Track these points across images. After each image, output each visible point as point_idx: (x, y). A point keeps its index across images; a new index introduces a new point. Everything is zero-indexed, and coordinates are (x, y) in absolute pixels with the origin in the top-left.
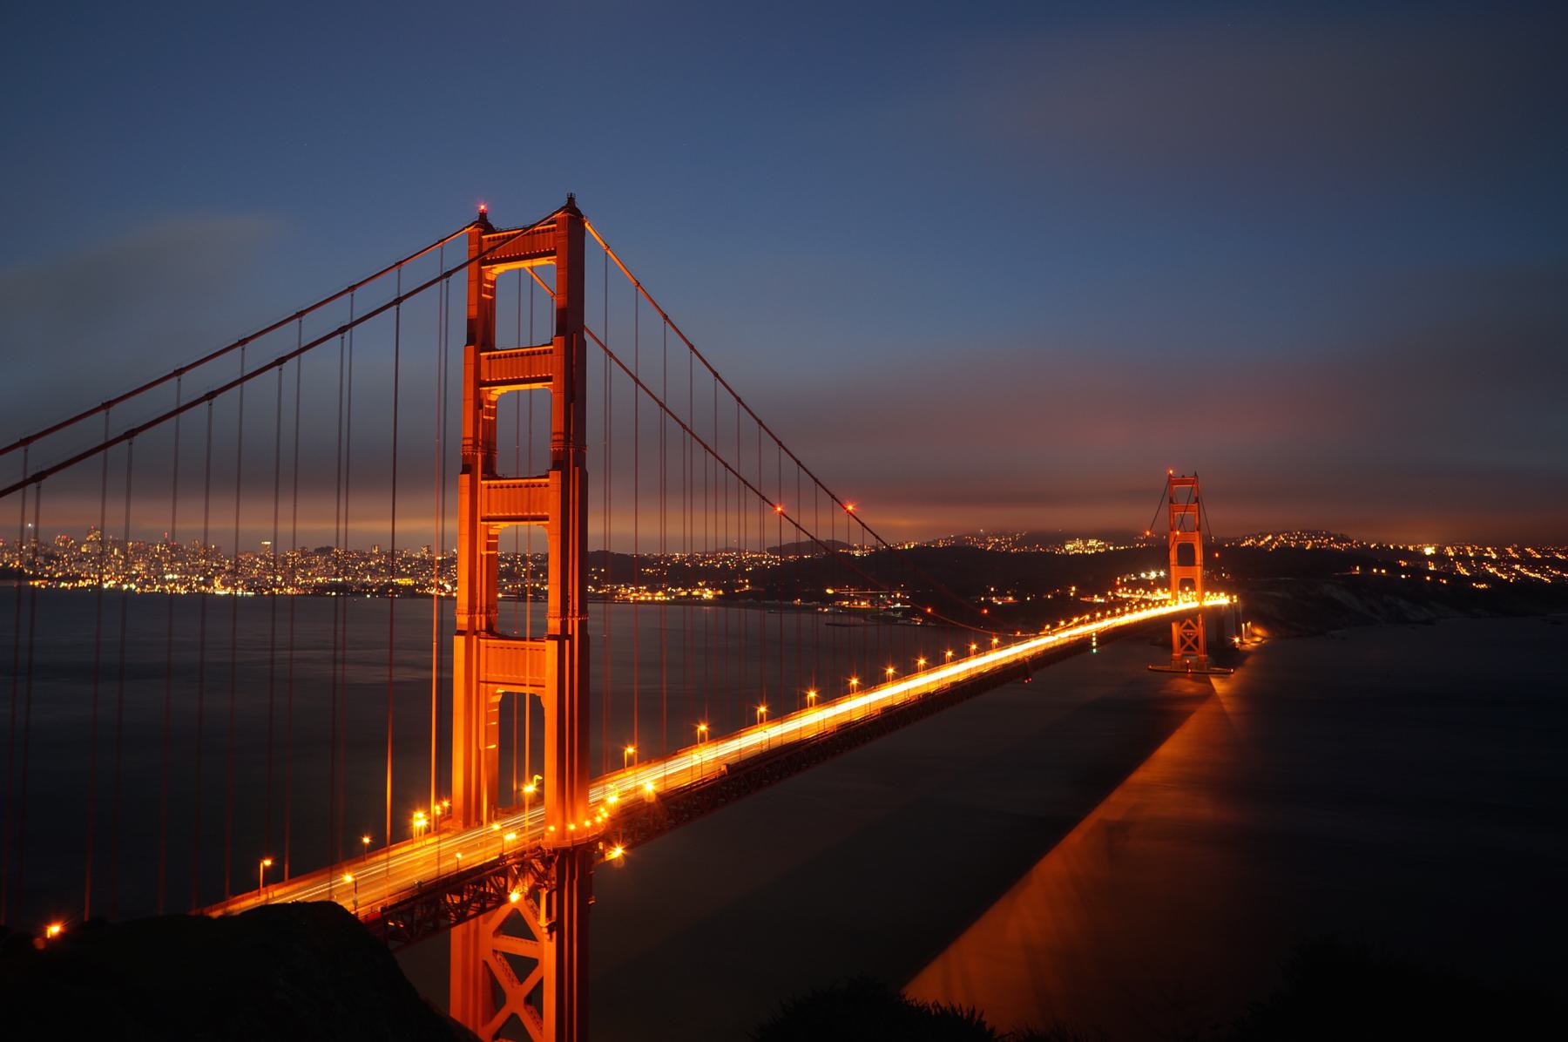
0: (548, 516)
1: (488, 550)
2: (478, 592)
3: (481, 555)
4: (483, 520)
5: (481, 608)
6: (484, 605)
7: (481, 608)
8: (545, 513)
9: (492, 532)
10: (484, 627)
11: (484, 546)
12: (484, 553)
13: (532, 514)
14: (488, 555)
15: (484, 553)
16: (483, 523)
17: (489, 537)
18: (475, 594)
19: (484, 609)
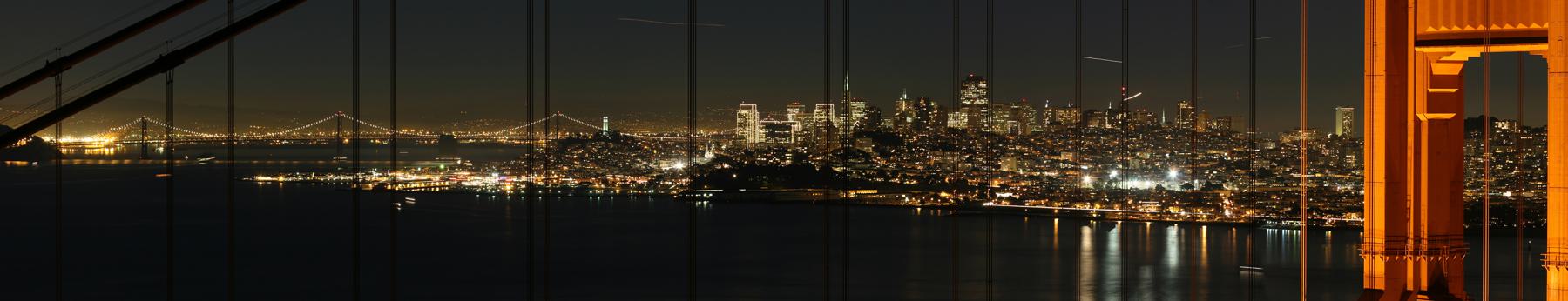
0: (1546, 31)
1: (1428, 112)
2: (1411, 204)
3: (1418, 122)
4: (1418, 43)
5: (1418, 239)
6: (1424, 235)
7: (1418, 239)
8: (1546, 26)
9: (1439, 69)
10: (1424, 284)
11: (1422, 102)
12: (1423, 117)
13: (1494, 27)
14: (1431, 121)
15: (1424, 117)
16: (1418, 49)
17: (1437, 81)
18: (1406, 210)
19: (1425, 245)
